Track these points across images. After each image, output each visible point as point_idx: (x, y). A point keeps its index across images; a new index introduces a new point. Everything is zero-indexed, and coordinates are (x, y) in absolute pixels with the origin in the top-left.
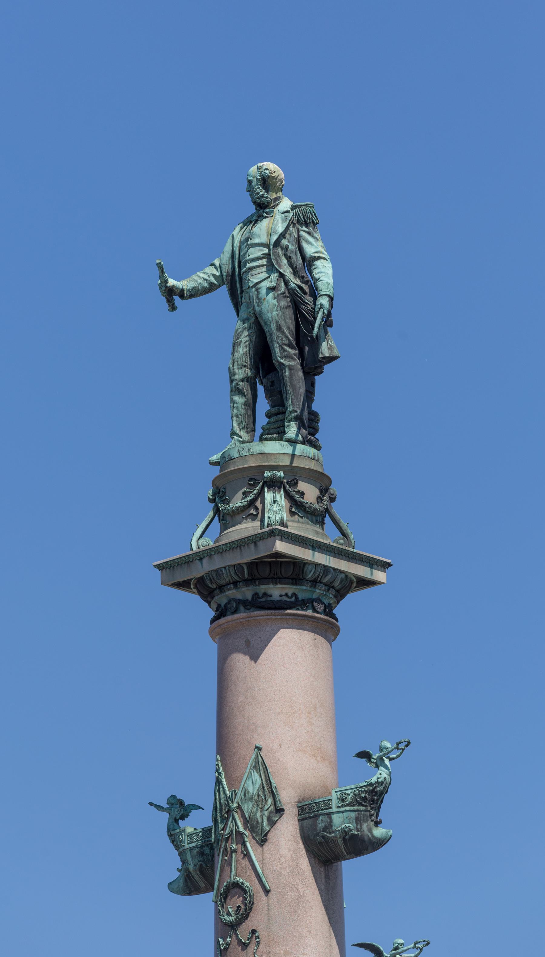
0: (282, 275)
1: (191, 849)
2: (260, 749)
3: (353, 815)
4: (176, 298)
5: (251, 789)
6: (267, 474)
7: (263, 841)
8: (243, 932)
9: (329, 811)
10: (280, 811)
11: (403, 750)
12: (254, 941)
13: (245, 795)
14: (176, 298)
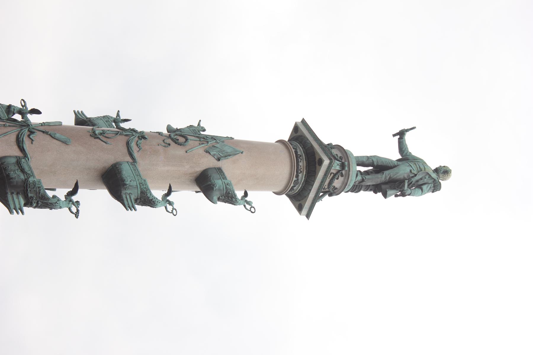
0: (416, 175)
2: (242, 153)
3: (222, 188)
4: (398, 137)
6: (346, 163)
11: (250, 210)
12: (166, 145)
14: (398, 137)
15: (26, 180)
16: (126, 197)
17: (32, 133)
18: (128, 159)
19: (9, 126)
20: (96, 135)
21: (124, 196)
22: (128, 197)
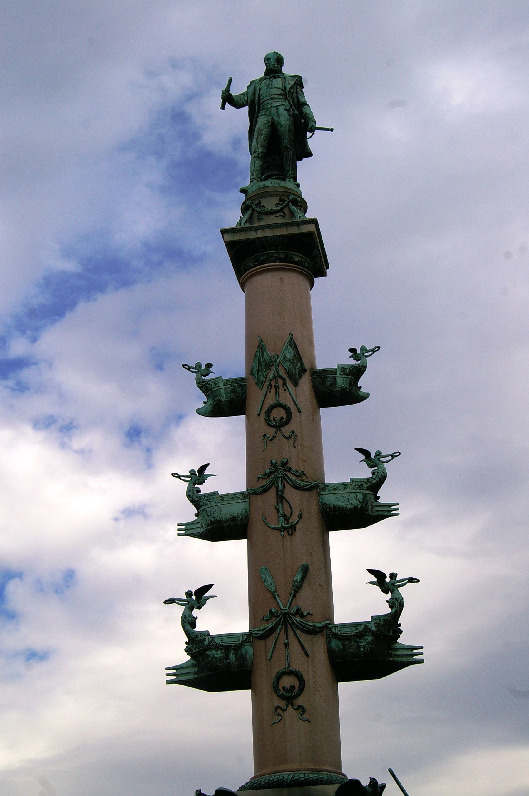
1: (225, 389)
5: (288, 356)
7: (296, 384)
8: (287, 430)
9: (334, 376)
10: (304, 371)
12: (293, 437)
13: (284, 358)
15: (373, 634)
16: (378, 511)
17: (299, 612)
18: (314, 493)
19: (287, 638)
20: (290, 527)
21: (376, 513)
22: (377, 509)
